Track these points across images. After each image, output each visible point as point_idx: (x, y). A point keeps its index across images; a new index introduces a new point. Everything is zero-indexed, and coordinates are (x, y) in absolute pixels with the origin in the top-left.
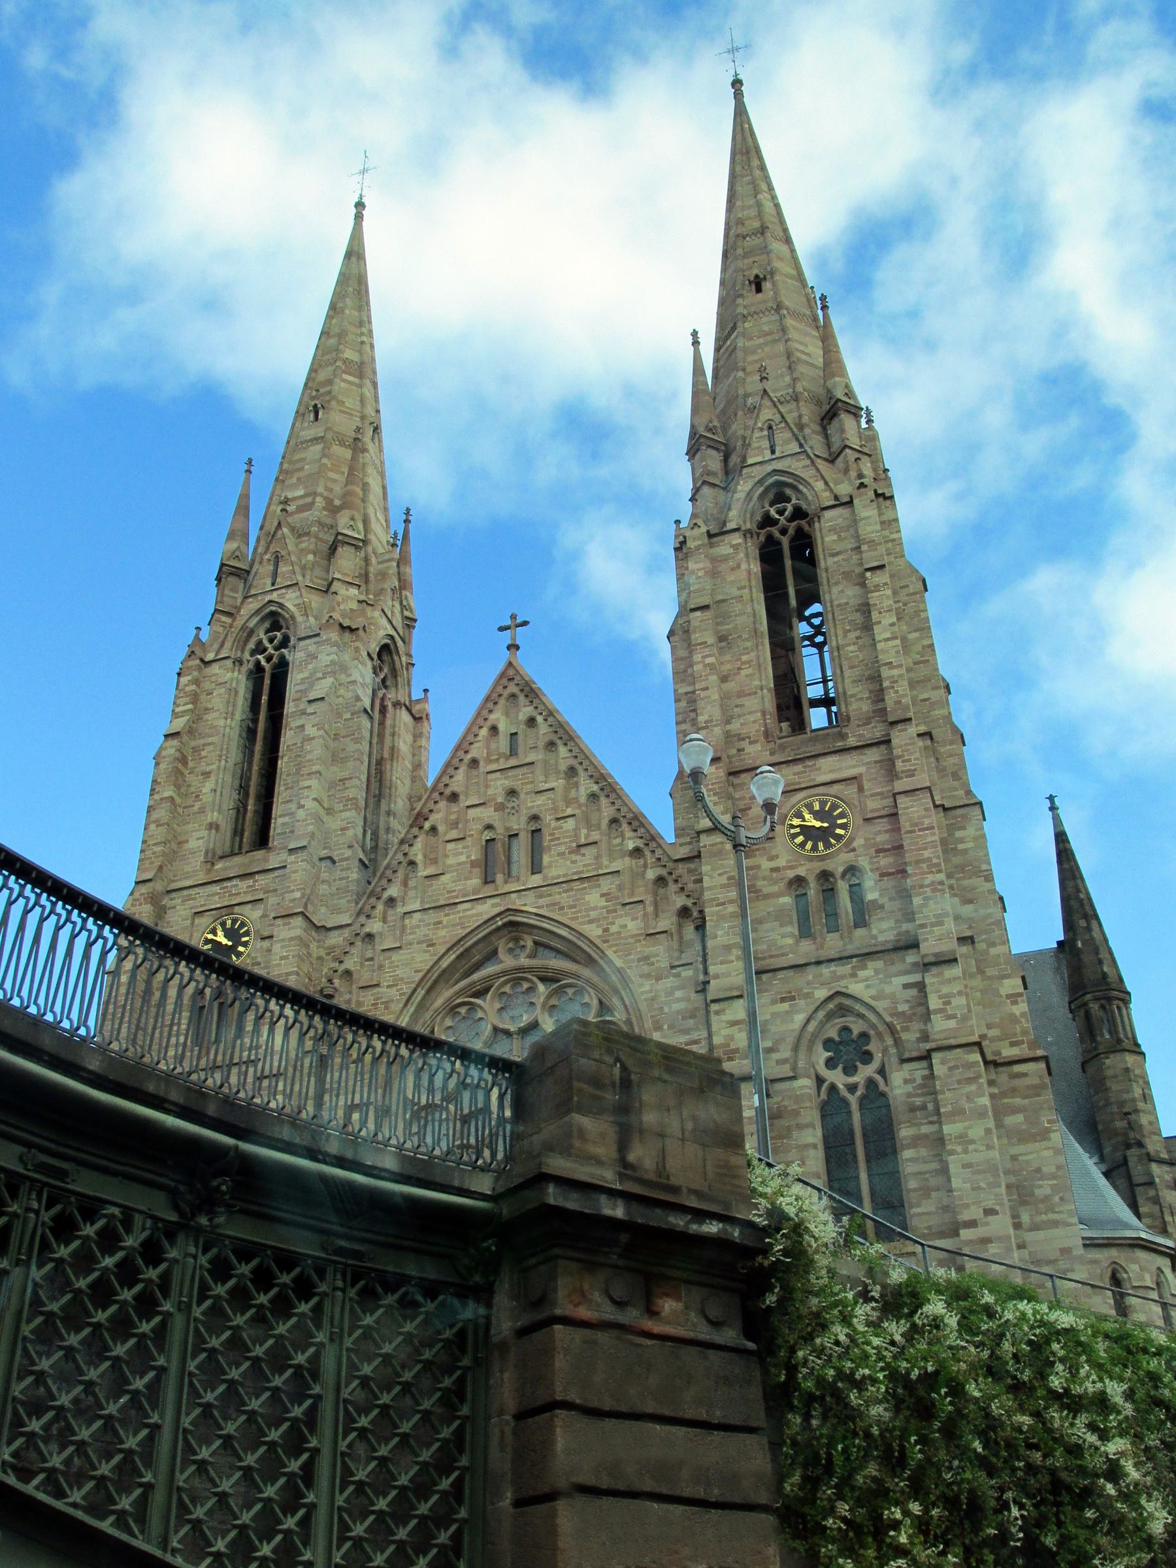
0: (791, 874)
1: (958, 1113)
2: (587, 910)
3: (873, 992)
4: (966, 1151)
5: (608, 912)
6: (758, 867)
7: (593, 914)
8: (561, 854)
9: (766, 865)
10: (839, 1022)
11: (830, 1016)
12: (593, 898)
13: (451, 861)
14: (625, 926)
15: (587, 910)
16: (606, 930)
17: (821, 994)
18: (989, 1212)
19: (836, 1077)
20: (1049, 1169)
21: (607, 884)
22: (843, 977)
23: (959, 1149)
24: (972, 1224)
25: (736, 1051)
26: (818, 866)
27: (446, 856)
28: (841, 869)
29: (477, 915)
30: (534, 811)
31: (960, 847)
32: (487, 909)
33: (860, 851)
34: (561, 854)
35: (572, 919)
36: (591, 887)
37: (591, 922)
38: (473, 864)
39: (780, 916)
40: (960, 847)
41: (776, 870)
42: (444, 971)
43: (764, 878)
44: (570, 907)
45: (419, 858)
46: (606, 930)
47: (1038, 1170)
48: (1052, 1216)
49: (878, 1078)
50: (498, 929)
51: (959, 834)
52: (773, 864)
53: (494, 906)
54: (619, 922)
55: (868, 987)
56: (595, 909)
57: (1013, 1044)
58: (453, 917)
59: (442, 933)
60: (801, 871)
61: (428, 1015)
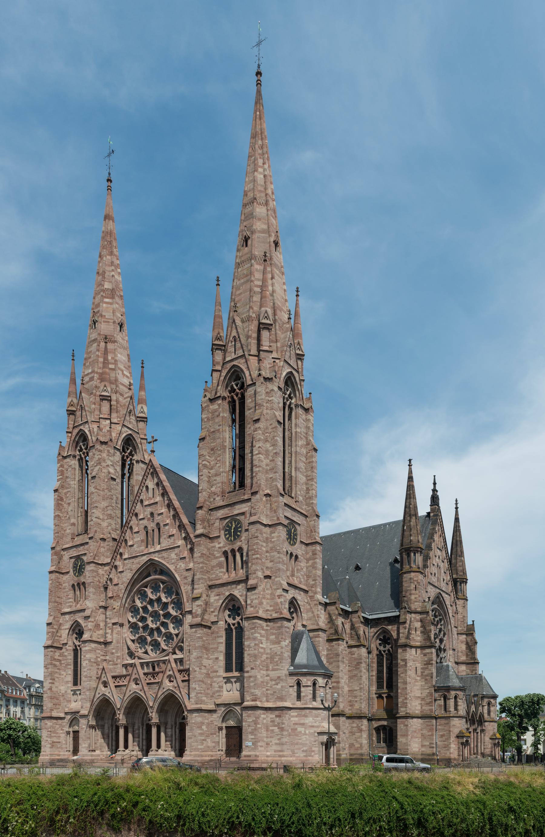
0: (224, 550)
1: (249, 638)
2: (172, 559)
3: (240, 594)
4: (249, 650)
5: (177, 560)
6: (215, 547)
7: (173, 561)
8: (165, 538)
9: (217, 546)
10: (232, 603)
11: (229, 601)
12: (173, 555)
13: (136, 540)
14: (181, 566)
15: (172, 559)
16: (176, 567)
17: (227, 594)
18: (252, 669)
19: (231, 621)
20: (279, 653)
21: (177, 550)
22: (233, 588)
23: (248, 649)
24: (248, 672)
25: (198, 615)
26: (231, 547)
27: (134, 538)
28: (237, 548)
29: (143, 560)
30: (158, 521)
31: (273, 540)
32: (145, 559)
33: (243, 541)
34: (165, 538)
35: (168, 563)
36: (173, 551)
37: (172, 564)
38: (142, 541)
39: (220, 565)
40: (273, 540)
41: (220, 548)
42: (135, 579)
43: (216, 551)
44: (168, 558)
45: (128, 538)
46: (176, 567)
47: (276, 653)
48: (277, 667)
49: (240, 621)
50: (149, 565)
51: (273, 535)
52: (219, 546)
53: (147, 557)
54: (180, 564)
55: (239, 592)
56: (173, 559)
57: (276, 613)
58: (137, 560)
59: (134, 566)
60: (226, 549)
61: (132, 594)
